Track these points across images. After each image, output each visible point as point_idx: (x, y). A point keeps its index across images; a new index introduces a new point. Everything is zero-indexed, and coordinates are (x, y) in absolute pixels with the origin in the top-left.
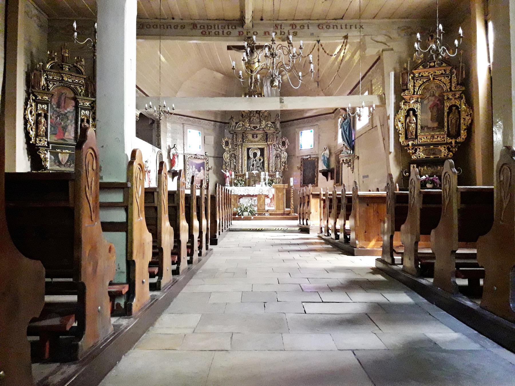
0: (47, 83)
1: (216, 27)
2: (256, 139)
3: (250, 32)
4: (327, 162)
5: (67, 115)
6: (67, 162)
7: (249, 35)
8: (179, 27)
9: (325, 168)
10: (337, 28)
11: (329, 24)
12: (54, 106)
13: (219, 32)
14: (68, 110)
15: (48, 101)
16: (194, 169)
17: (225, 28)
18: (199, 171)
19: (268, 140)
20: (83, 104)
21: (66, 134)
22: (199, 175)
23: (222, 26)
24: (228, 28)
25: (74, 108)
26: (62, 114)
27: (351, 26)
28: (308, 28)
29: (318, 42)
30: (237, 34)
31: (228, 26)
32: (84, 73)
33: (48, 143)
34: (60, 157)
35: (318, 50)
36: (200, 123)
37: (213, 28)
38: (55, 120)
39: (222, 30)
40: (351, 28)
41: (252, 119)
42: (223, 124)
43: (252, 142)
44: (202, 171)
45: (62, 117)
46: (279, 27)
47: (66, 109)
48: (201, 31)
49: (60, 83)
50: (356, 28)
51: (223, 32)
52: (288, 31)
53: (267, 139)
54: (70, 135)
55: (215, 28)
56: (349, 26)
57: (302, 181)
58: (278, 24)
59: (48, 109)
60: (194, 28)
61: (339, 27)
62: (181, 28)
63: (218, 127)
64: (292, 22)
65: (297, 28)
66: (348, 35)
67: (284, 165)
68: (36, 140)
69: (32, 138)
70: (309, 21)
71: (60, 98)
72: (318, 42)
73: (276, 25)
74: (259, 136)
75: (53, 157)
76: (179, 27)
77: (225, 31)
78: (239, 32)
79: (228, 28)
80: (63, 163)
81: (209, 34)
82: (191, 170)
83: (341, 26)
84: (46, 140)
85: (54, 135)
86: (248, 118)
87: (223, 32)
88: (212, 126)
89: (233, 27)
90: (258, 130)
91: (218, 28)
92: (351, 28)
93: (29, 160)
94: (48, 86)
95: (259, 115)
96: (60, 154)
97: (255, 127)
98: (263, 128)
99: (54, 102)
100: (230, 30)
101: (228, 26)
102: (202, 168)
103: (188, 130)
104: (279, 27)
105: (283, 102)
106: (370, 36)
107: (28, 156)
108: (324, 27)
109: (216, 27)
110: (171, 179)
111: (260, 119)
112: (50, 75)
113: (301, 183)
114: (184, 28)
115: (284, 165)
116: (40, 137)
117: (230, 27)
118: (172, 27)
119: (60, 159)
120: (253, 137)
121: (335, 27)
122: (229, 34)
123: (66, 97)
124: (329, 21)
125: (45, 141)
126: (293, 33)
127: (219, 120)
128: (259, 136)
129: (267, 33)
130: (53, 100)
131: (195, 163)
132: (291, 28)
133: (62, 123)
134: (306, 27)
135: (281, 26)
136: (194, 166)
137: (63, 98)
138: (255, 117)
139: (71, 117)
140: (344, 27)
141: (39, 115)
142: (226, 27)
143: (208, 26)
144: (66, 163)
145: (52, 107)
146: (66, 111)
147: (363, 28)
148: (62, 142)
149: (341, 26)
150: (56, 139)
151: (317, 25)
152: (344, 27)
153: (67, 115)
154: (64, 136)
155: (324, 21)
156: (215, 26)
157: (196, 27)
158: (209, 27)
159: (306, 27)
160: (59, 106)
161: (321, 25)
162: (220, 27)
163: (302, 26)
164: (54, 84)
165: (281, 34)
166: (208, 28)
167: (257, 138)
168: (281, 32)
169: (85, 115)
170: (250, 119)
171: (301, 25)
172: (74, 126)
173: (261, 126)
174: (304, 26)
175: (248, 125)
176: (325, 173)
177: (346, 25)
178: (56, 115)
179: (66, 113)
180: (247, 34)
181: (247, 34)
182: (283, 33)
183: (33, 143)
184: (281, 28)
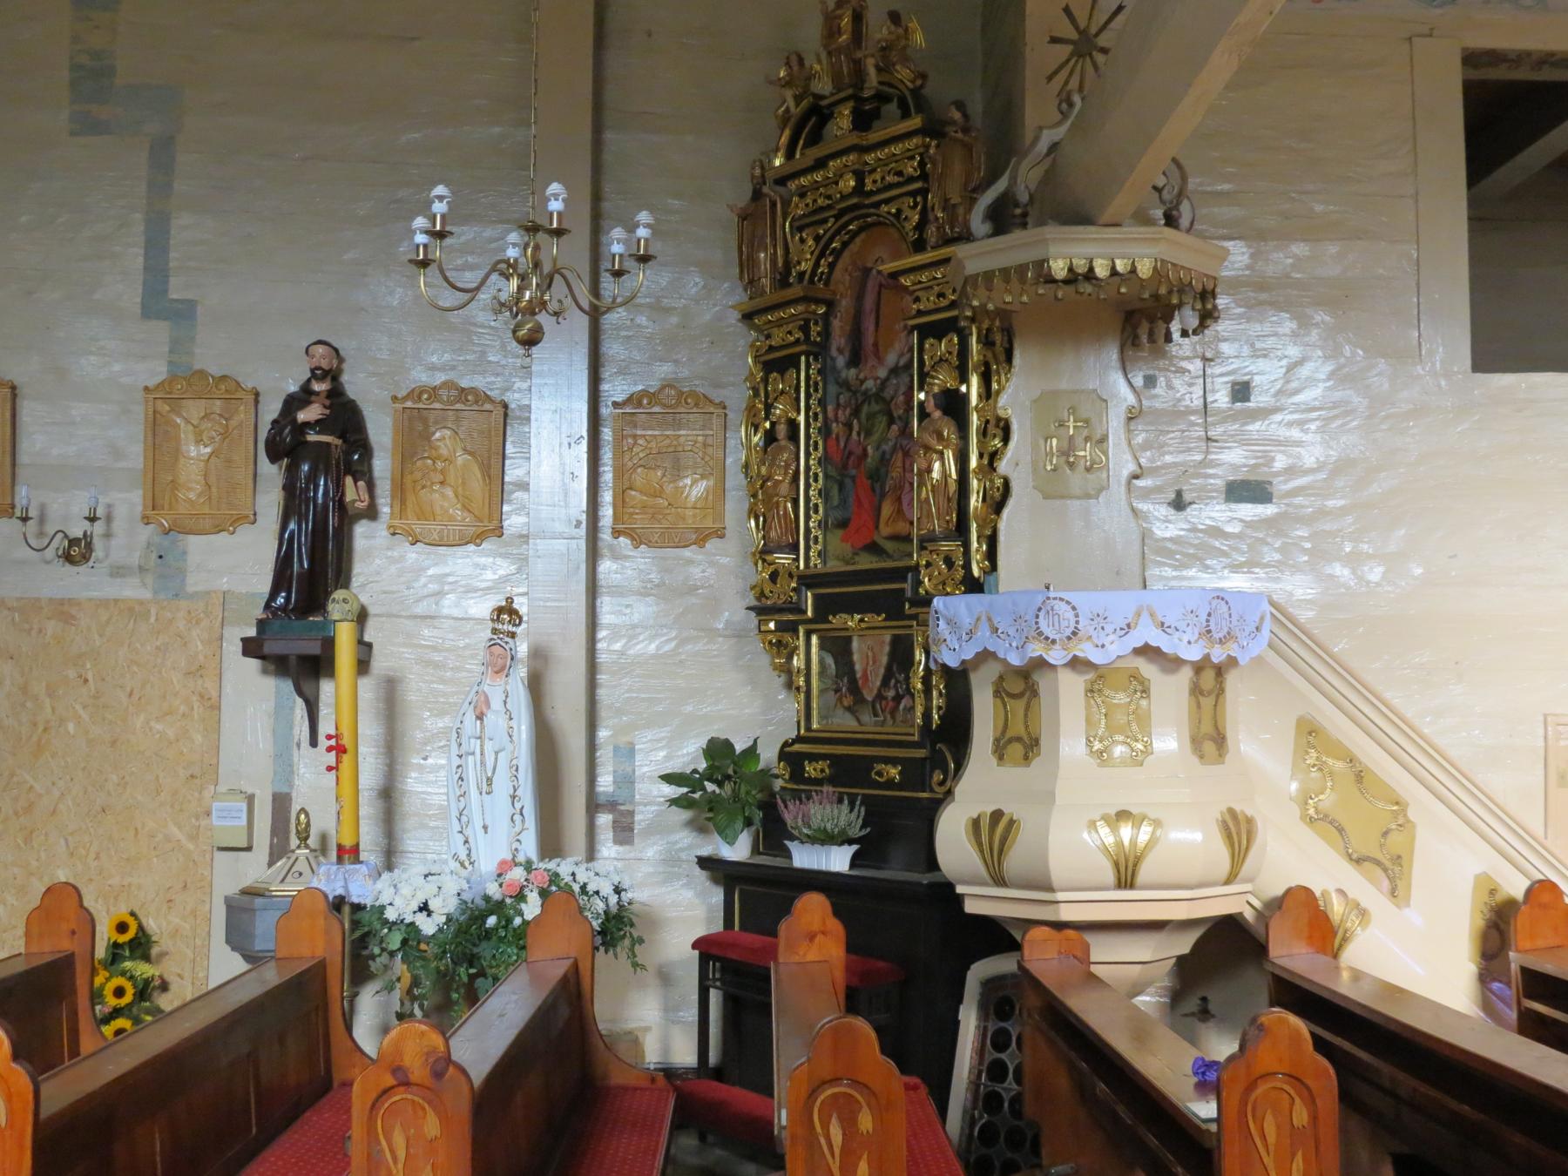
34: (856, 657)
47: (880, 360)
49: (837, 217)
130: (836, 323)
133: (870, 450)
144: (879, 690)
148: (866, 563)
153: (888, 394)
154: (877, 527)
160: (855, 360)
164: (817, 239)
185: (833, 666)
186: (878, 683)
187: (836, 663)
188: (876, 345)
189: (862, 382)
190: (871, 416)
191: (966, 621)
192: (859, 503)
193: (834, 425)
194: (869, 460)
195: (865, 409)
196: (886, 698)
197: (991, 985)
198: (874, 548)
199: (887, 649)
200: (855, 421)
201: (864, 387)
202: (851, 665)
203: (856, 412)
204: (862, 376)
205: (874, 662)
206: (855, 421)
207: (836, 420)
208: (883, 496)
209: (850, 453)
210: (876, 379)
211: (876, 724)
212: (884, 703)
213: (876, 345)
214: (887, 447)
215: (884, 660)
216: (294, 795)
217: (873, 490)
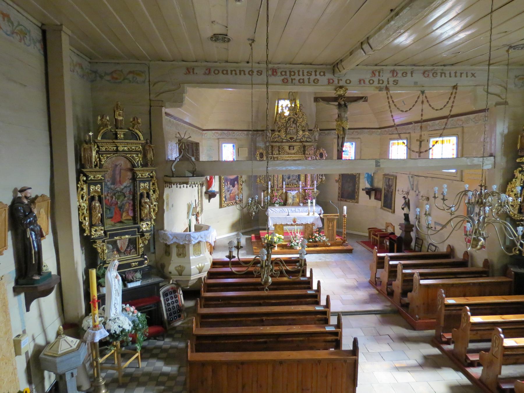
0: (99, 158)
1: (301, 73)
2: (293, 151)
3: (341, 80)
4: (371, 179)
5: (124, 191)
6: (127, 247)
7: (342, 83)
8: (255, 73)
9: (368, 186)
10: (445, 76)
11: (437, 71)
12: (108, 183)
13: (303, 79)
14: (125, 184)
15: (101, 179)
16: (229, 185)
17: (311, 75)
18: (234, 186)
19: (306, 152)
20: (142, 175)
21: (124, 214)
22: (234, 190)
23: (308, 72)
24: (316, 75)
25: (131, 181)
26: (118, 192)
27: (461, 74)
28: (412, 76)
29: (423, 92)
30: (326, 82)
31: (316, 72)
32: (142, 138)
33: (105, 232)
34: (118, 244)
35: (423, 102)
36: (234, 135)
37: (297, 74)
38: (110, 201)
39: (308, 77)
40: (461, 77)
41: (288, 130)
42: (255, 132)
43: (288, 154)
44: (236, 186)
45: (118, 196)
46: (377, 74)
47: (121, 184)
48: (283, 77)
50: (467, 77)
51: (309, 79)
52: (388, 79)
53: (304, 151)
54: (128, 215)
55: (299, 75)
56: (459, 74)
57: (340, 195)
58: (376, 70)
59: (101, 189)
60: (273, 74)
61: (448, 75)
62: (257, 74)
63: (250, 136)
64: (392, 68)
65: (398, 75)
66: (458, 85)
67: (321, 177)
68: (90, 231)
69: (86, 229)
70: (413, 67)
71: (114, 171)
72: (423, 92)
73: (373, 72)
74: (296, 148)
75: (110, 246)
76: (255, 73)
77: (313, 77)
78: (329, 80)
79: (316, 75)
80: (122, 251)
81: (292, 82)
82: (226, 187)
83: (450, 74)
84: (103, 228)
85: (110, 219)
86: (285, 129)
87: (309, 79)
88: (245, 136)
89: (322, 74)
90: (295, 141)
91: (303, 75)
92: (461, 77)
93: (83, 253)
94: (100, 161)
95: (296, 125)
96: (118, 242)
97: (291, 138)
98: (300, 139)
99: (108, 178)
100: (318, 77)
101: (316, 72)
102: (236, 182)
103: (223, 145)
104: (377, 74)
105: (379, 166)
106: (483, 87)
107: (82, 250)
108: (431, 75)
109: (301, 73)
110: (207, 200)
111: (297, 130)
112: (102, 146)
113: (339, 196)
114: (261, 74)
115: (321, 177)
116: (95, 227)
117: (318, 73)
118: (247, 73)
119: (119, 246)
120: (290, 149)
121: (443, 75)
122: (316, 81)
123: (121, 169)
124: (436, 68)
125: (102, 230)
126: (394, 81)
127: (251, 129)
128: (296, 148)
129: (362, 82)
131: (230, 179)
132: (391, 75)
133: (119, 202)
134: (409, 75)
135: (379, 72)
136: (229, 183)
137: (117, 172)
138: (291, 127)
139: (128, 192)
140: (453, 75)
141: (92, 199)
142: (313, 73)
143: (290, 72)
144: (126, 249)
145: (106, 185)
146: (122, 187)
147: (475, 77)
149: (450, 74)
150: (113, 223)
151: (422, 72)
152: (453, 75)
154: (121, 217)
155: (432, 68)
156: (299, 71)
157: (276, 72)
158: (293, 74)
159: (409, 75)
160: (113, 183)
161: (427, 73)
162: (305, 74)
163: (404, 74)
164: (107, 157)
165: (379, 83)
166: (290, 75)
167: (294, 149)
168: (379, 80)
169: (145, 188)
170: (286, 129)
171: (403, 71)
172: (131, 202)
173: (298, 137)
174: (406, 73)
175: (284, 136)
176: (368, 192)
177: (456, 73)
178: (111, 194)
179: (123, 189)
180: (338, 83)
181: (338, 83)
182: (381, 82)
183: (87, 235)
184: (379, 76)
185: (112, 247)
186: (125, 248)
187: (112, 246)
188: (120, 181)
189: (116, 188)
190: (119, 196)
191: (196, 237)
192: (116, 213)
193: (107, 197)
194: (119, 204)
195: (117, 194)
196: (128, 251)
197: (163, 293)
198: (121, 222)
199: (127, 241)
200: (114, 196)
201: (116, 189)
202: (117, 246)
203: (114, 194)
204: (115, 187)
205: (124, 244)
206: (114, 196)
207: (108, 195)
208: (123, 211)
209: (112, 204)
210: (120, 188)
211: (125, 256)
212: (127, 252)
213: (120, 181)
214: (124, 202)
215: (127, 243)
216: (26, 329)
217: (120, 210)
